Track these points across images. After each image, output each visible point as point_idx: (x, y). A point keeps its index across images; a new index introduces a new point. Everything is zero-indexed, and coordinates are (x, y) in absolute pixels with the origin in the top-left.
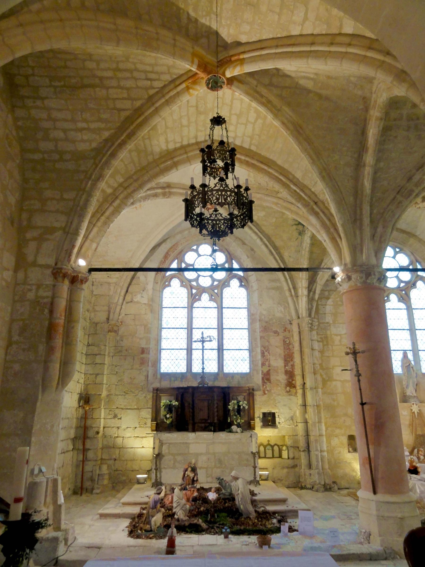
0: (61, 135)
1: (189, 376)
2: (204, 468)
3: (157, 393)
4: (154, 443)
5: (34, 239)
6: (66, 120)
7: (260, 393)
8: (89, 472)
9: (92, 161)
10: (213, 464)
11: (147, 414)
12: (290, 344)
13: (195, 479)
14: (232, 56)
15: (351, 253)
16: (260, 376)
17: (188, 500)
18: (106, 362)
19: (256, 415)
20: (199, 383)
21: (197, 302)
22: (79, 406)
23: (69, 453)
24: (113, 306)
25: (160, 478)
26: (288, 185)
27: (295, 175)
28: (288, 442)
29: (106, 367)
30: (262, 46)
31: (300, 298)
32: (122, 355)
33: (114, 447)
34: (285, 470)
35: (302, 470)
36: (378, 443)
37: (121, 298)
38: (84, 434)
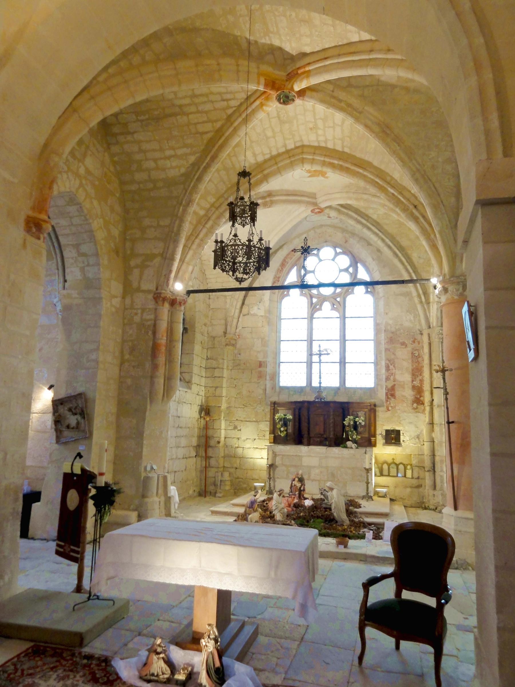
0: (152, 164)
1: (308, 389)
2: (316, 480)
3: (275, 406)
4: (268, 454)
5: (137, 266)
6: (154, 150)
7: (384, 409)
8: (212, 477)
10: (326, 477)
11: (265, 427)
12: (419, 356)
13: (302, 489)
14: (299, 68)
16: (384, 391)
17: (289, 506)
18: (225, 375)
19: (378, 432)
20: (316, 398)
21: (318, 312)
22: (201, 417)
23: (191, 459)
24: (229, 319)
26: (385, 188)
27: (393, 176)
28: (414, 462)
29: (225, 380)
30: (326, 57)
31: (431, 304)
32: (240, 369)
33: (234, 457)
34: (409, 490)
35: (426, 491)
36: (462, 462)
37: (237, 311)
38: (205, 443)
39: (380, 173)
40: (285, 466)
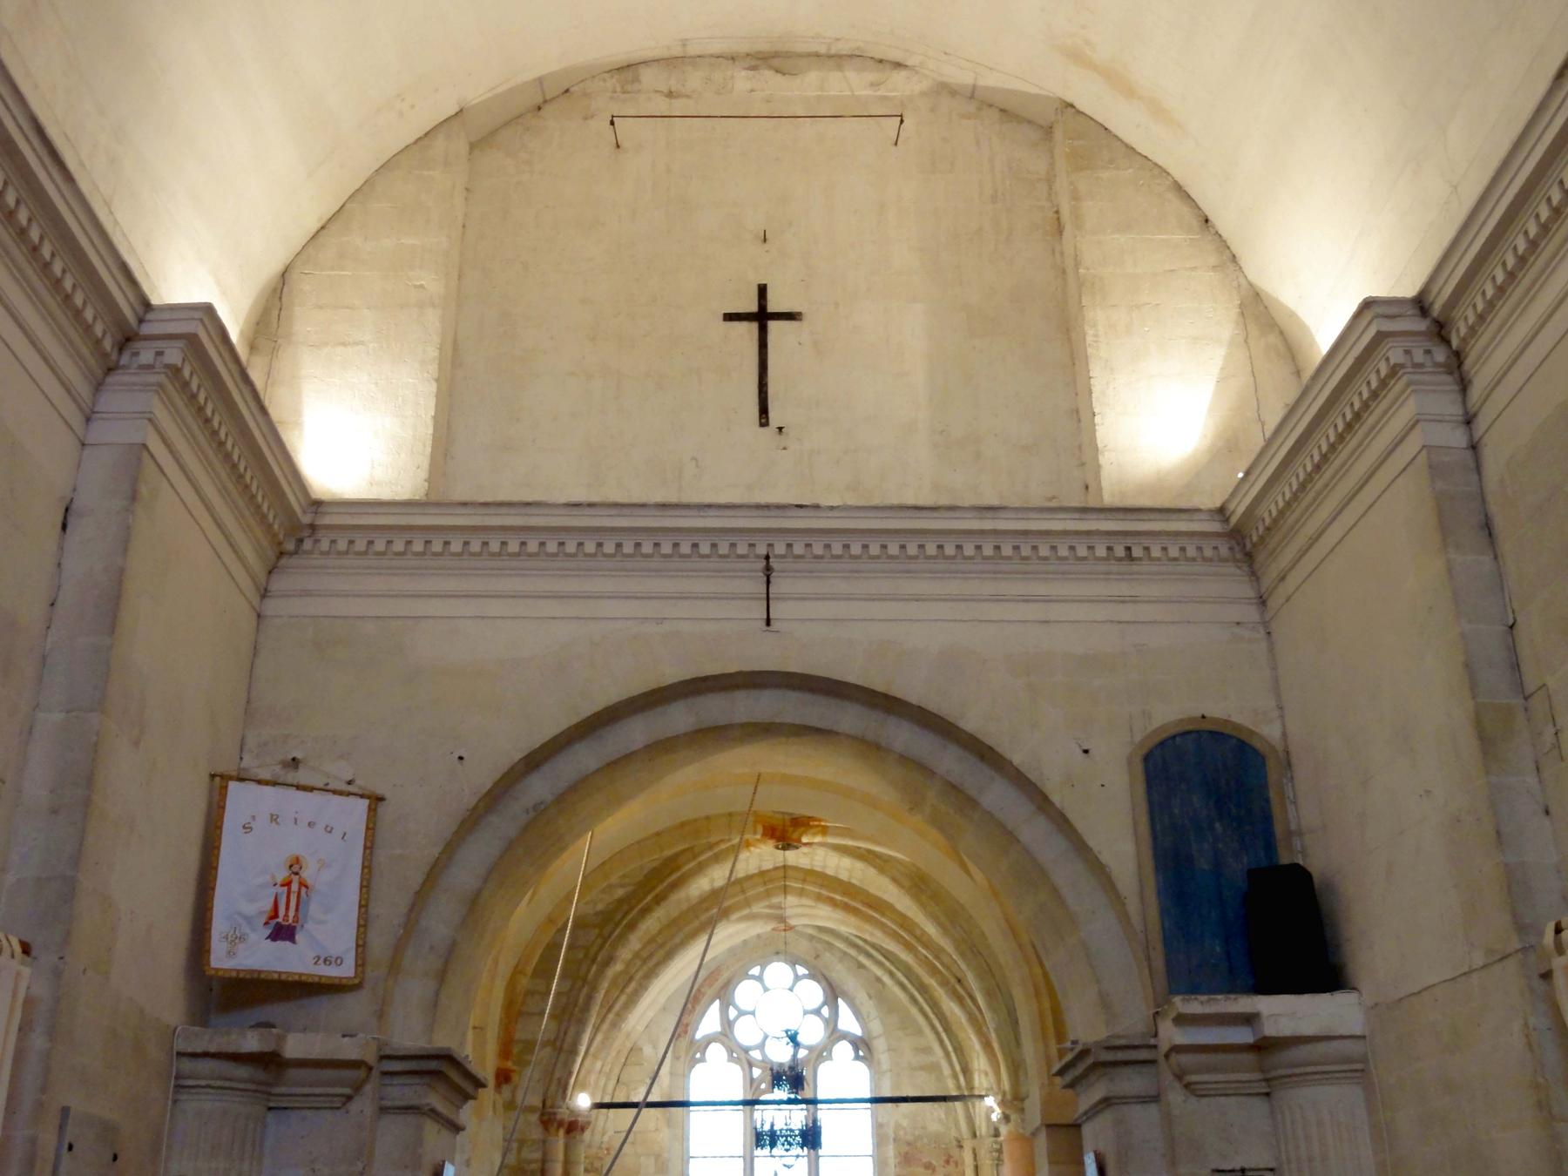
9: (597, 931)
15: (1010, 1075)
39: (905, 922)
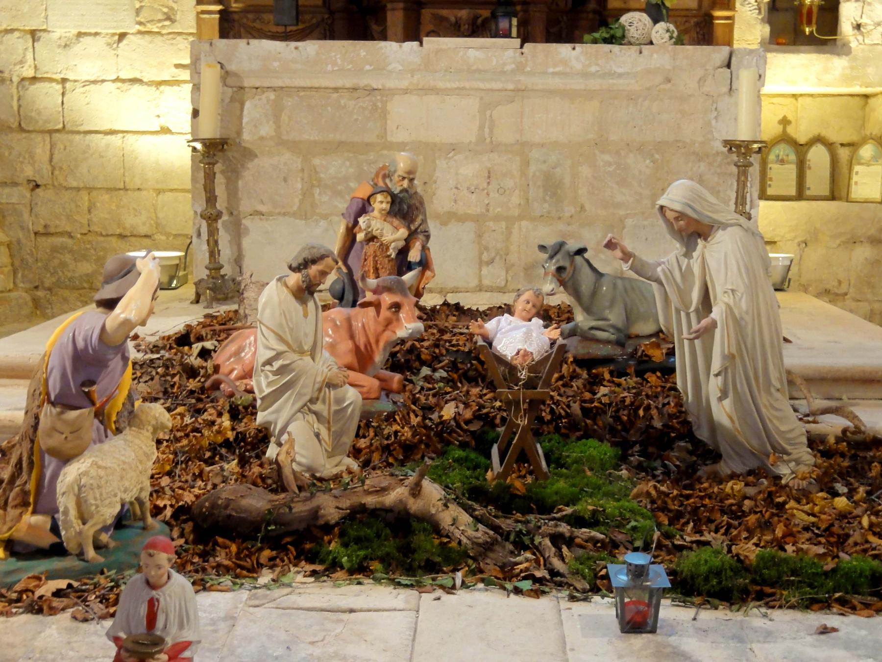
2: (462, 219)
4: (196, 88)
10: (516, 199)
13: (414, 255)
17: (362, 360)
25: (238, 261)
33: (21, 129)
34: (863, 253)
40: (294, 146)
